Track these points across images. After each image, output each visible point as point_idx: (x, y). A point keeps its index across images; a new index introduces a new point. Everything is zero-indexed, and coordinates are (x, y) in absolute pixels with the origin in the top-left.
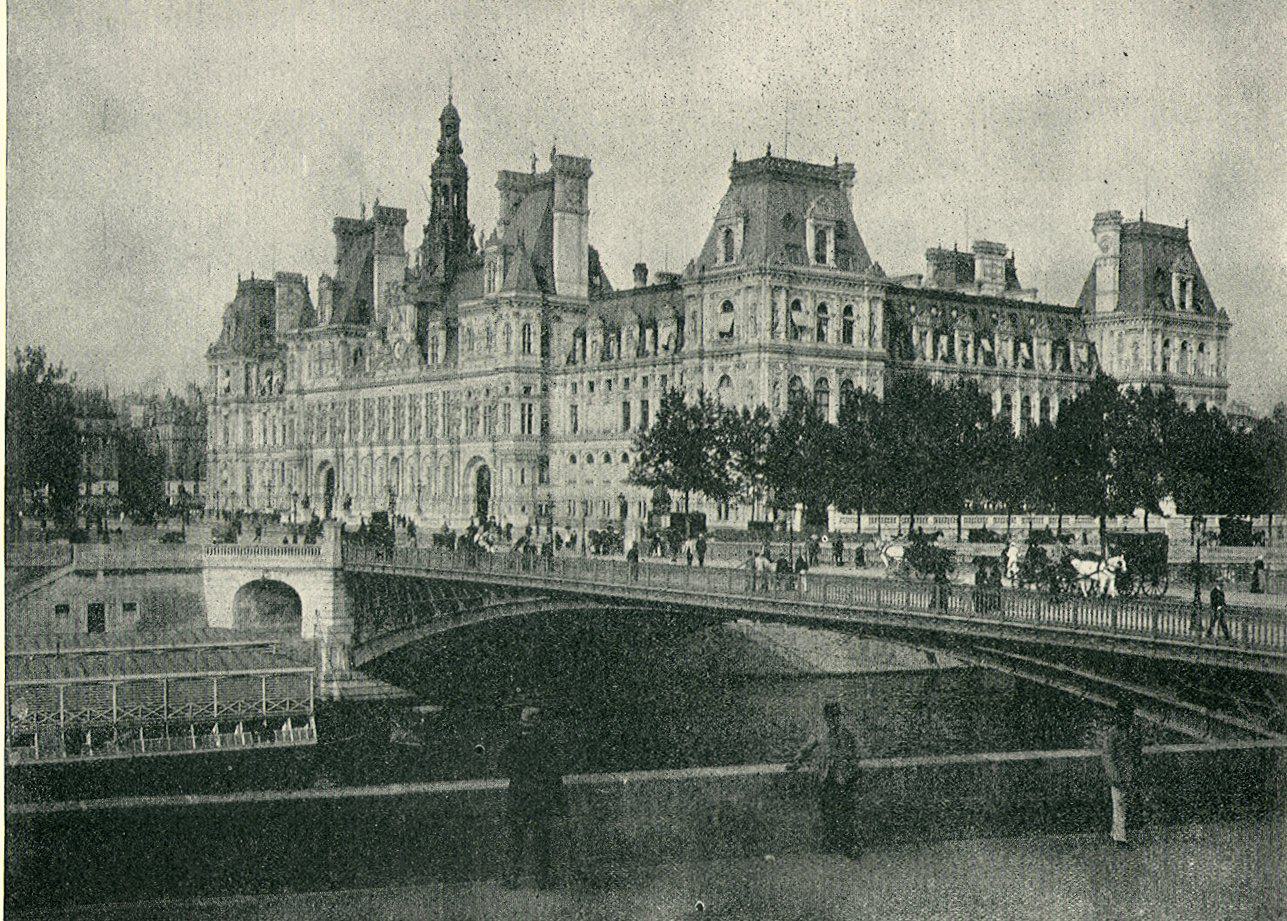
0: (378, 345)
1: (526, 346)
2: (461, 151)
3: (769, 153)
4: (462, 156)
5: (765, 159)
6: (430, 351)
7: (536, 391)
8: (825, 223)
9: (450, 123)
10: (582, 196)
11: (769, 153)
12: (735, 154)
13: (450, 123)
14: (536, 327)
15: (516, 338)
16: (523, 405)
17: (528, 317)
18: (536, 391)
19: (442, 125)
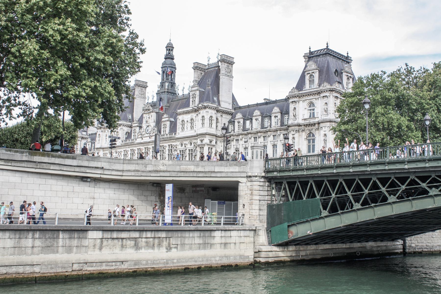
0: (137, 129)
1: (211, 124)
2: (173, 59)
3: (327, 46)
4: (174, 61)
5: (325, 49)
6: (162, 129)
7: (213, 143)
8: (349, 75)
9: (170, 48)
10: (231, 71)
11: (327, 46)
12: (310, 48)
13: (170, 48)
14: (214, 118)
15: (207, 121)
16: (209, 148)
17: (212, 113)
18: (213, 143)
19: (167, 50)
